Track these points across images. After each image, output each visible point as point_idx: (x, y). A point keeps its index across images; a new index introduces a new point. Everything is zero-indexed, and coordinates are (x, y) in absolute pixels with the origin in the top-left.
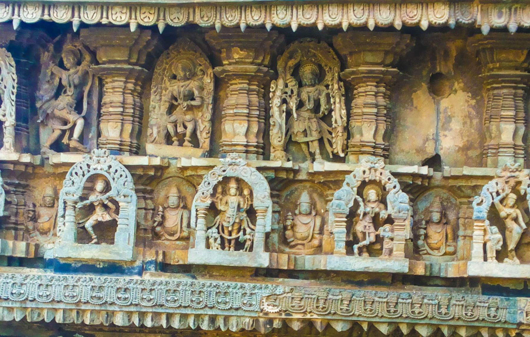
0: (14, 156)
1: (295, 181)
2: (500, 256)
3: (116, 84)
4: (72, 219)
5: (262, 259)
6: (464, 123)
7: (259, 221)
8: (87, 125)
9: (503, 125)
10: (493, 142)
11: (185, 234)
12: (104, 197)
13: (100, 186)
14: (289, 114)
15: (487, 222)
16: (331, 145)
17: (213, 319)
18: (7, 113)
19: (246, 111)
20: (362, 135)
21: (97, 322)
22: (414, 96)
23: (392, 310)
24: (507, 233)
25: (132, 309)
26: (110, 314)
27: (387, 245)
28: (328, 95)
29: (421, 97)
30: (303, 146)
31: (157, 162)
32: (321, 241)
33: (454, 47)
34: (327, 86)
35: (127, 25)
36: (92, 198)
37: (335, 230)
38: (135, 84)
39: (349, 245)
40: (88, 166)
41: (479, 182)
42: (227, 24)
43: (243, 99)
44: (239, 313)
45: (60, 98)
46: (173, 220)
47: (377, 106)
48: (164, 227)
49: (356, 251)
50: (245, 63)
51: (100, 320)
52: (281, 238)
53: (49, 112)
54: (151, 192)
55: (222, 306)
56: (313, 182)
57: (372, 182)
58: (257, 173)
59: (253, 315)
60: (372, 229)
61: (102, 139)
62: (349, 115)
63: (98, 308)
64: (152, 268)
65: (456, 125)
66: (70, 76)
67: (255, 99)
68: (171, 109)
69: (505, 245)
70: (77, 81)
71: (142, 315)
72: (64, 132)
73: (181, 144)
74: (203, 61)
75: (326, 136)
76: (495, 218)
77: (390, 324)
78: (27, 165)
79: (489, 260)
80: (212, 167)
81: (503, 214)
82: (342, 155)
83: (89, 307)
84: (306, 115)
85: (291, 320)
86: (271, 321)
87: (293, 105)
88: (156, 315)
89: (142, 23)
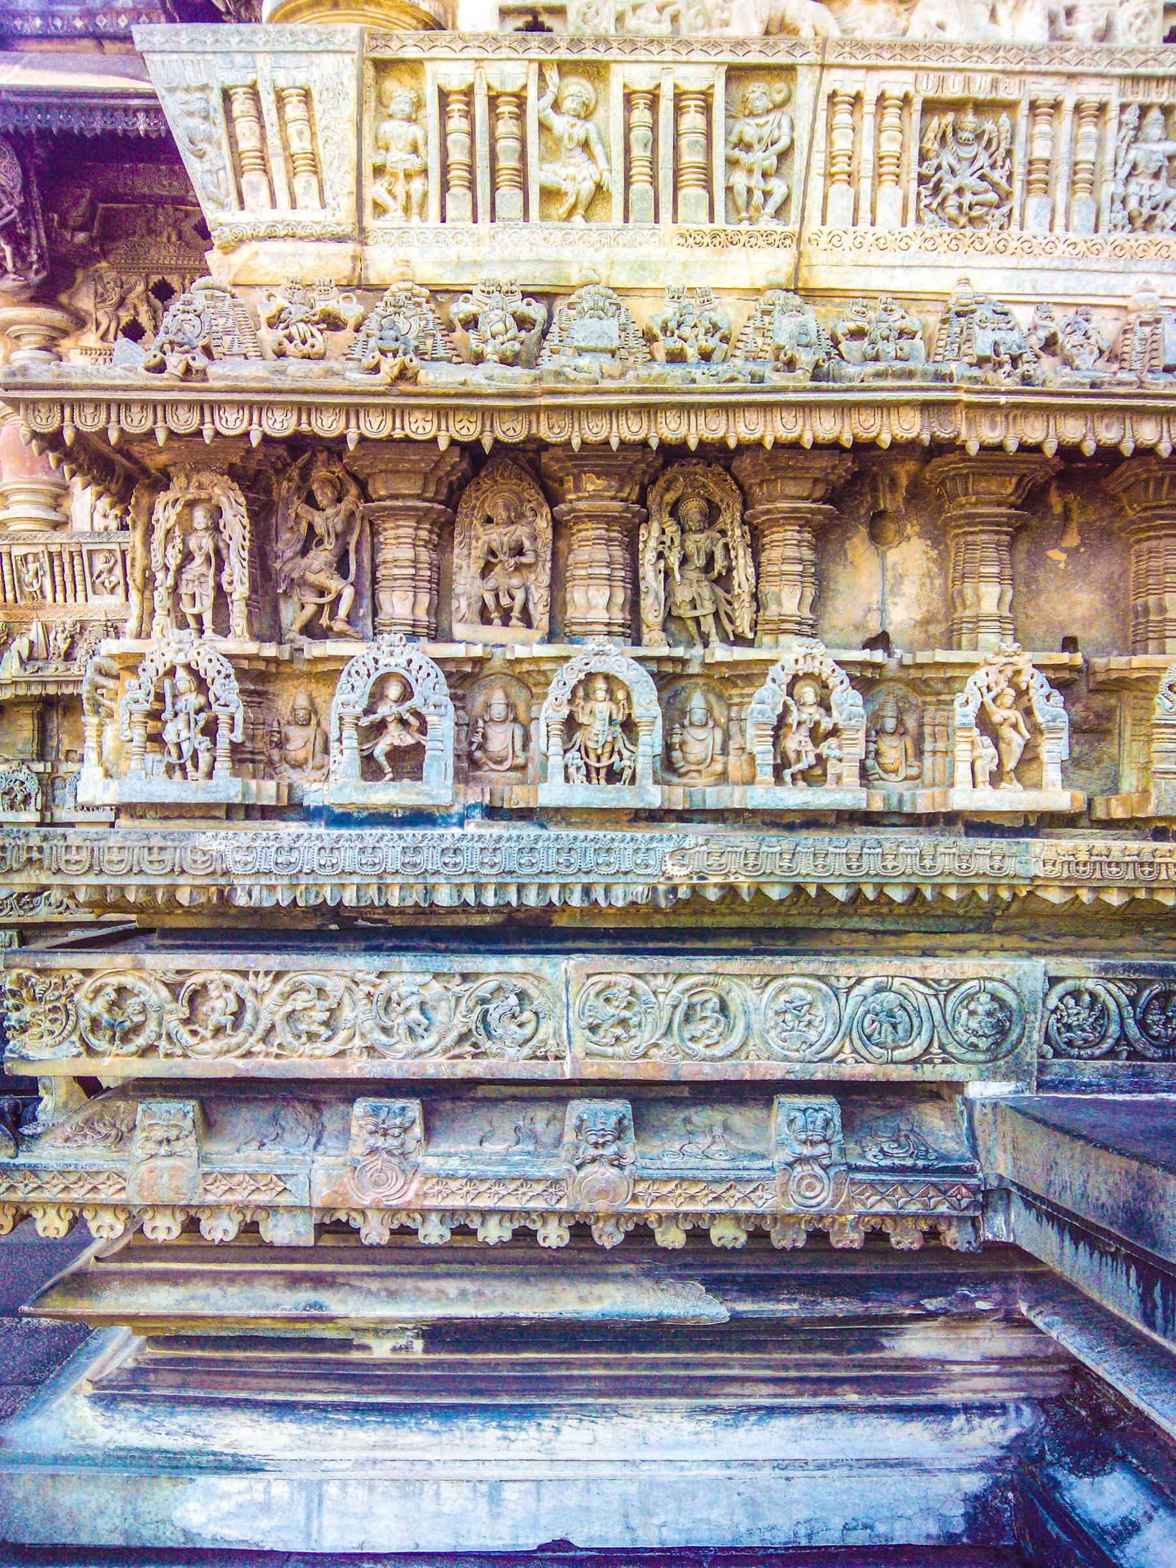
0: (252, 648)
1: (681, 676)
2: (996, 778)
3: (401, 531)
4: (355, 744)
5: (653, 797)
6: (923, 585)
7: (643, 738)
8: (358, 594)
9: (983, 588)
10: (968, 613)
11: (520, 761)
12: (403, 709)
13: (394, 691)
14: (668, 573)
15: (976, 731)
16: (732, 622)
17: (587, 890)
18: (236, 578)
19: (607, 571)
20: (780, 604)
21: (409, 902)
22: (847, 545)
23: (855, 865)
24: (1002, 745)
25: (466, 879)
26: (429, 890)
27: (833, 768)
28: (726, 546)
29: (859, 545)
30: (690, 623)
31: (477, 651)
32: (725, 764)
33: (904, 471)
34: (723, 533)
35: (434, 440)
36: (384, 710)
37: (755, 750)
38: (431, 532)
39: (778, 771)
40: (376, 661)
41: (957, 673)
42: (591, 438)
43: (601, 554)
44: (628, 879)
45: (311, 554)
46: (500, 739)
47: (801, 561)
48: (485, 751)
49: (788, 778)
50: (602, 498)
51: (415, 897)
52: (668, 765)
53: (295, 575)
54: (462, 698)
55: (604, 870)
56: (708, 676)
57: (808, 676)
58: (636, 665)
59: (650, 880)
60: (810, 746)
61: (382, 617)
62: (758, 577)
63: (412, 880)
64: (477, 813)
65: (910, 588)
66: (327, 520)
67: (618, 553)
68: (486, 570)
69: (1000, 765)
70: (339, 528)
71: (479, 888)
72: (321, 607)
73: (506, 623)
74: (533, 495)
75: (725, 607)
76: (984, 723)
77: (848, 885)
78: (268, 660)
79: (980, 786)
80: (567, 659)
81: (996, 718)
82: (750, 636)
83: (399, 879)
84: (694, 575)
85: (704, 886)
86: (674, 890)
87: (674, 559)
88: (501, 887)
89: (457, 437)
